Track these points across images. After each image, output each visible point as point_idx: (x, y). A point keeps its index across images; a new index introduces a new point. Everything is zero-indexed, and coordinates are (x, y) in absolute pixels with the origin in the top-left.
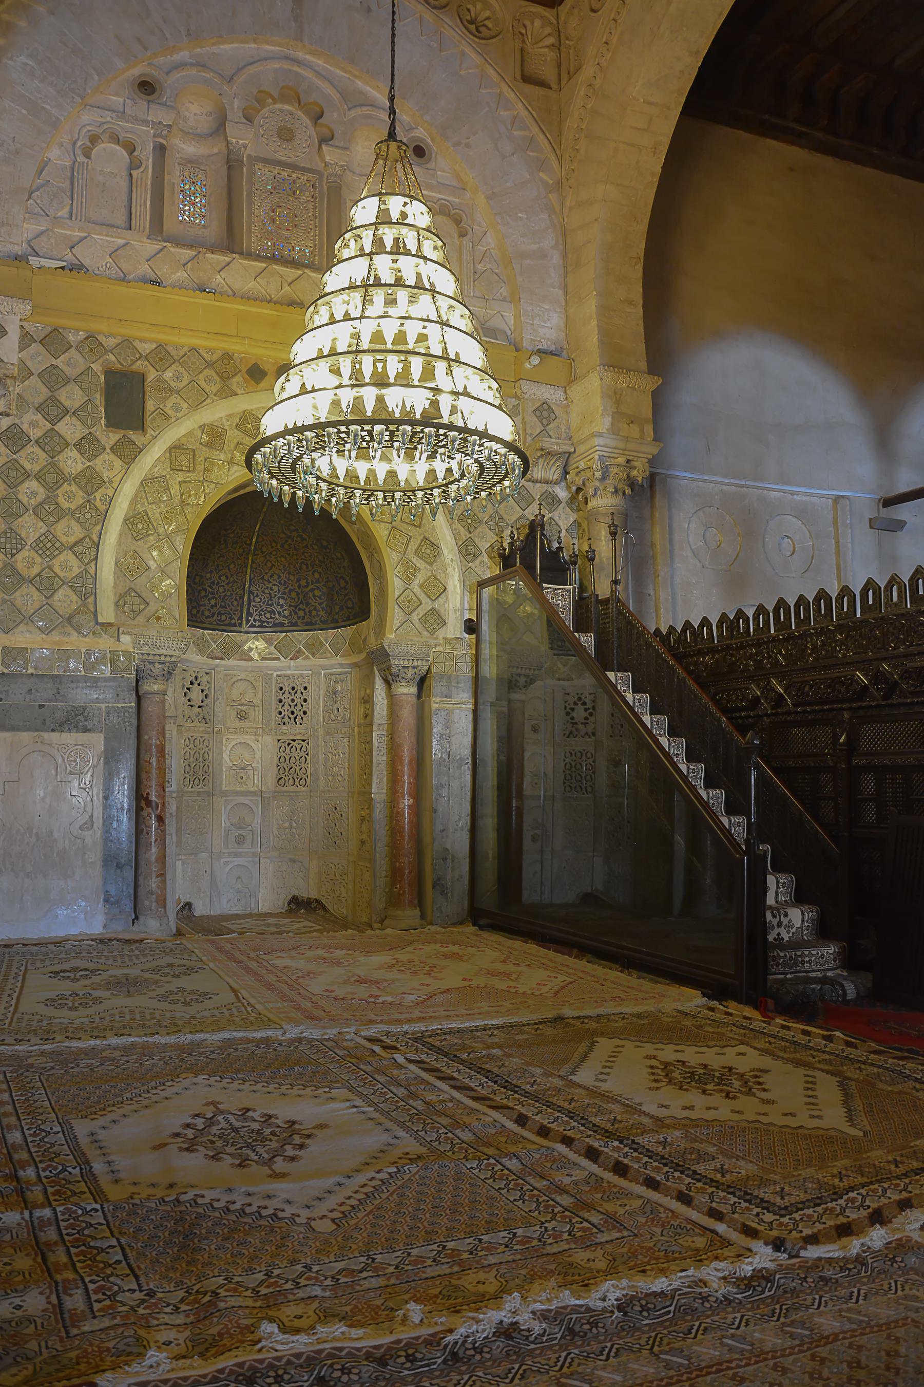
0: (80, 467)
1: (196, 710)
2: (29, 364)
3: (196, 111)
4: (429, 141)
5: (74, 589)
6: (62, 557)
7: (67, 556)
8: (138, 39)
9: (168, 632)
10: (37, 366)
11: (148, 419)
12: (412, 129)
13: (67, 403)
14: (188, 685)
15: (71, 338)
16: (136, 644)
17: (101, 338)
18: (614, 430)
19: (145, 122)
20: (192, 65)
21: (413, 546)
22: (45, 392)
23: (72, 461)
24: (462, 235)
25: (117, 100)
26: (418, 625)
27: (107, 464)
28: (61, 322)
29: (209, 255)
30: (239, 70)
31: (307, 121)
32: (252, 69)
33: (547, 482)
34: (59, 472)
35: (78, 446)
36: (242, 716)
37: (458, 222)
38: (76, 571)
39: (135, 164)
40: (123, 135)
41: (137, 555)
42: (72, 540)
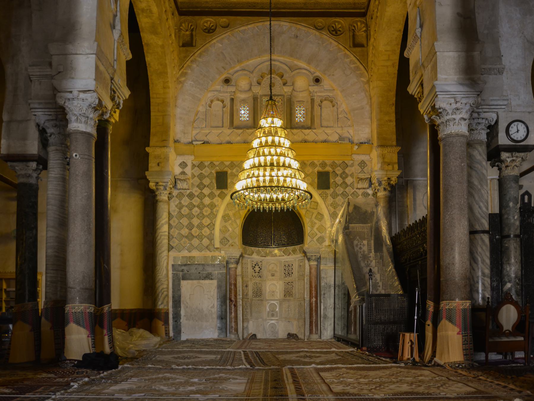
0: (209, 202)
1: (257, 273)
2: (195, 173)
3: (244, 84)
4: (321, 76)
5: (208, 238)
6: (205, 229)
7: (206, 229)
8: (223, 67)
9: (236, 249)
10: (196, 174)
11: (228, 185)
12: (315, 73)
13: (205, 184)
14: (254, 265)
15: (206, 164)
16: (226, 253)
17: (215, 163)
18: (382, 169)
19: (227, 92)
20: (241, 70)
21: (314, 216)
22: (199, 181)
23: (207, 201)
24: (333, 106)
25: (218, 87)
26: (316, 242)
27: (217, 200)
28: (203, 159)
29: (247, 131)
30: (255, 68)
31: (279, 79)
32: (259, 67)
33: (364, 189)
34: (203, 204)
35: (209, 196)
36: (273, 275)
37: (332, 102)
38: (208, 233)
39: (224, 107)
40: (220, 98)
41: (225, 227)
42: (207, 224)
